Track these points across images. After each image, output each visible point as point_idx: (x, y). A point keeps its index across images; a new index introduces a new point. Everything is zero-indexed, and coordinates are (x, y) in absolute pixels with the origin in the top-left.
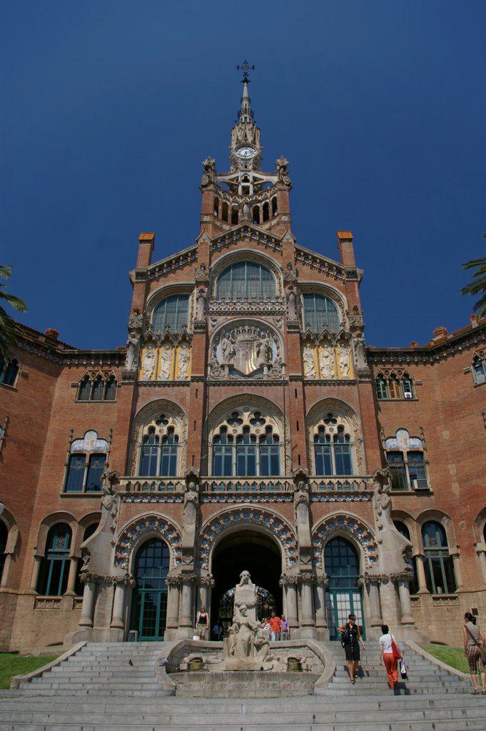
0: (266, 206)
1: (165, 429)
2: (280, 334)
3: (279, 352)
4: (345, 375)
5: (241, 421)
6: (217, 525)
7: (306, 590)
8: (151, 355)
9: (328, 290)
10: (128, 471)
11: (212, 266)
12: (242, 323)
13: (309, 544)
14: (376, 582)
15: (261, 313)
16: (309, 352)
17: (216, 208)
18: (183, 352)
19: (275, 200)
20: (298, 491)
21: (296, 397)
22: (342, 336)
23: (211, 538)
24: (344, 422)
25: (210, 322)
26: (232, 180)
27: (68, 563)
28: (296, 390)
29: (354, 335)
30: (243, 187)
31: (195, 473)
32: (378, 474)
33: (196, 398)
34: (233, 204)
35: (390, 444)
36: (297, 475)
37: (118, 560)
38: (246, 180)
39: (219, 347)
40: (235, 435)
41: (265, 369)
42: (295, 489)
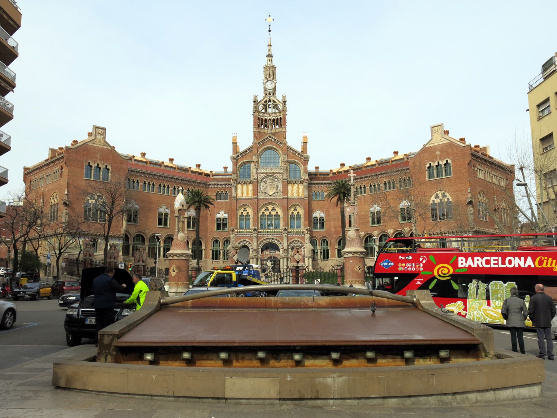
0: (277, 119)
3: (280, 187)
5: (268, 210)
10: (237, 228)
15: (274, 173)
18: (251, 187)
19: (281, 118)
22: (301, 182)
23: (260, 245)
25: (258, 176)
26: (264, 102)
27: (219, 251)
30: (269, 105)
35: (315, 215)
38: (270, 101)
39: (261, 184)
40: (267, 215)
41: (276, 193)
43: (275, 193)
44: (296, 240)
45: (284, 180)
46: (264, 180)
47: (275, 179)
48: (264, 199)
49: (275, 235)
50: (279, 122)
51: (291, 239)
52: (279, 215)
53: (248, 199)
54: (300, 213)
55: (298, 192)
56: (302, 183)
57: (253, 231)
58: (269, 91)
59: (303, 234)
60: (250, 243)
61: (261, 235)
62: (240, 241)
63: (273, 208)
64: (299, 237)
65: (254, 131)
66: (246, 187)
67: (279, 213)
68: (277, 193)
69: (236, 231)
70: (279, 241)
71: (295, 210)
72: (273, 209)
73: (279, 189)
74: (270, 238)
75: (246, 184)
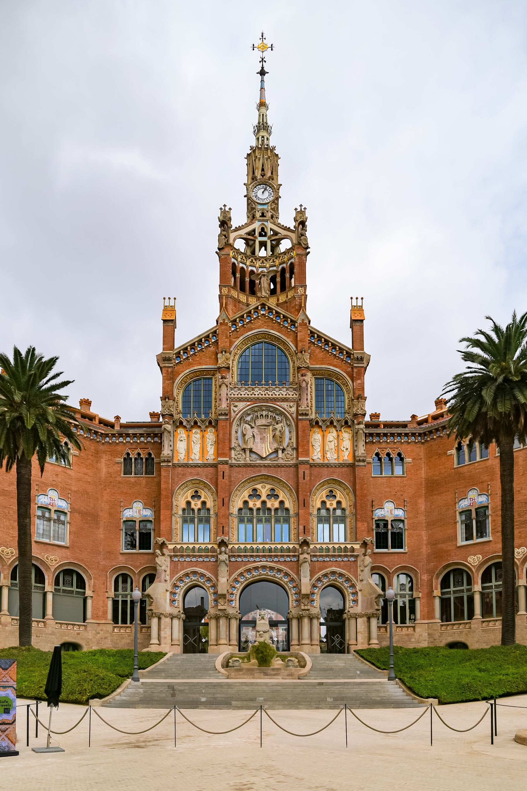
0: (283, 270)
1: (199, 503)
2: (293, 419)
4: (346, 458)
5: (259, 496)
6: (242, 577)
7: (306, 621)
8: (182, 439)
9: (338, 376)
11: (232, 349)
12: (260, 408)
13: (309, 592)
14: (356, 617)
15: (275, 400)
16: (316, 437)
17: (234, 274)
20: (302, 554)
21: (304, 479)
22: (346, 422)
24: (342, 498)
25: (232, 407)
28: (304, 472)
29: (356, 422)
31: (225, 541)
32: (364, 541)
33: (223, 478)
34: (250, 268)
36: (302, 542)
37: (173, 601)
38: (263, 231)
40: (255, 509)
41: (280, 452)
42: (300, 552)
43: (276, 451)
44: (333, 573)
45: (302, 414)
46: (248, 418)
47: (277, 417)
48: (246, 466)
49: (276, 559)
50: (288, 275)
51: (321, 569)
52: (287, 510)
53: (205, 466)
54: (344, 505)
55: (338, 449)
56: (350, 427)
57: (216, 547)
58: (260, 207)
59: (351, 556)
60: (209, 580)
61: (239, 559)
62: (182, 572)
63: (273, 489)
64: (342, 563)
65: (221, 297)
66: (198, 436)
67: (287, 505)
68: (283, 450)
69: (171, 547)
70: (287, 574)
71: (331, 495)
72: (273, 495)
73: (286, 441)
74: (264, 567)
75: (200, 427)
